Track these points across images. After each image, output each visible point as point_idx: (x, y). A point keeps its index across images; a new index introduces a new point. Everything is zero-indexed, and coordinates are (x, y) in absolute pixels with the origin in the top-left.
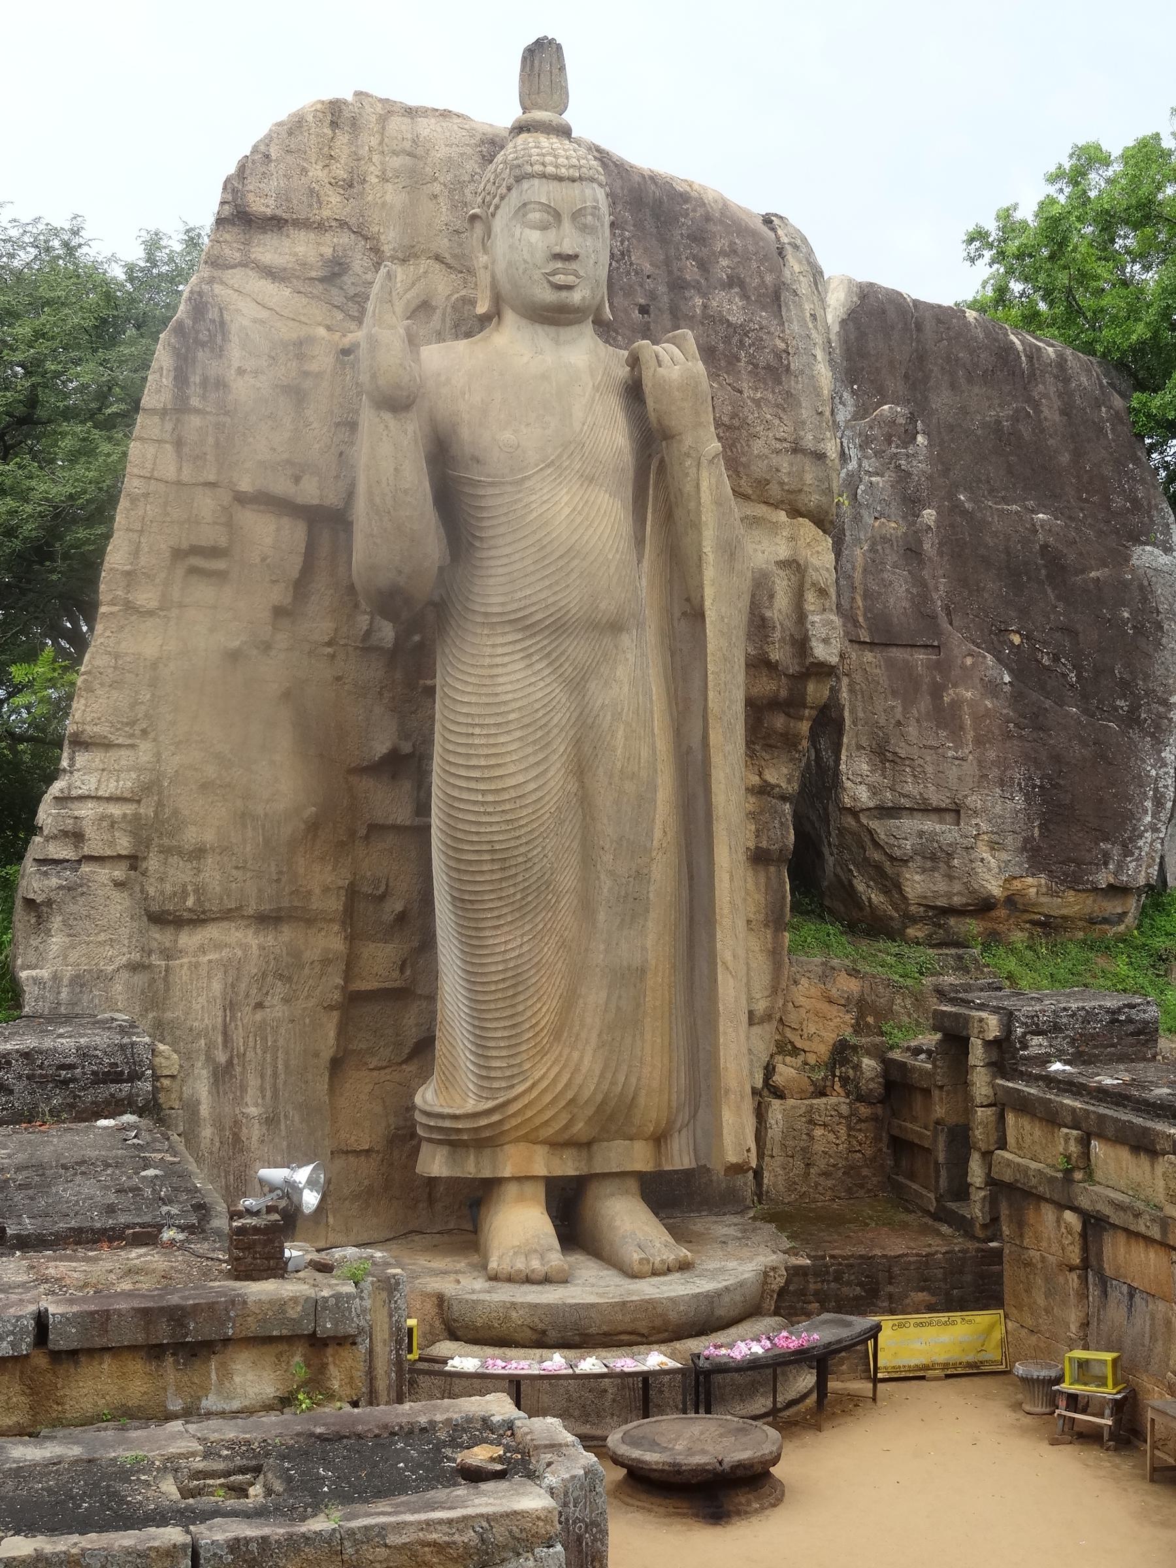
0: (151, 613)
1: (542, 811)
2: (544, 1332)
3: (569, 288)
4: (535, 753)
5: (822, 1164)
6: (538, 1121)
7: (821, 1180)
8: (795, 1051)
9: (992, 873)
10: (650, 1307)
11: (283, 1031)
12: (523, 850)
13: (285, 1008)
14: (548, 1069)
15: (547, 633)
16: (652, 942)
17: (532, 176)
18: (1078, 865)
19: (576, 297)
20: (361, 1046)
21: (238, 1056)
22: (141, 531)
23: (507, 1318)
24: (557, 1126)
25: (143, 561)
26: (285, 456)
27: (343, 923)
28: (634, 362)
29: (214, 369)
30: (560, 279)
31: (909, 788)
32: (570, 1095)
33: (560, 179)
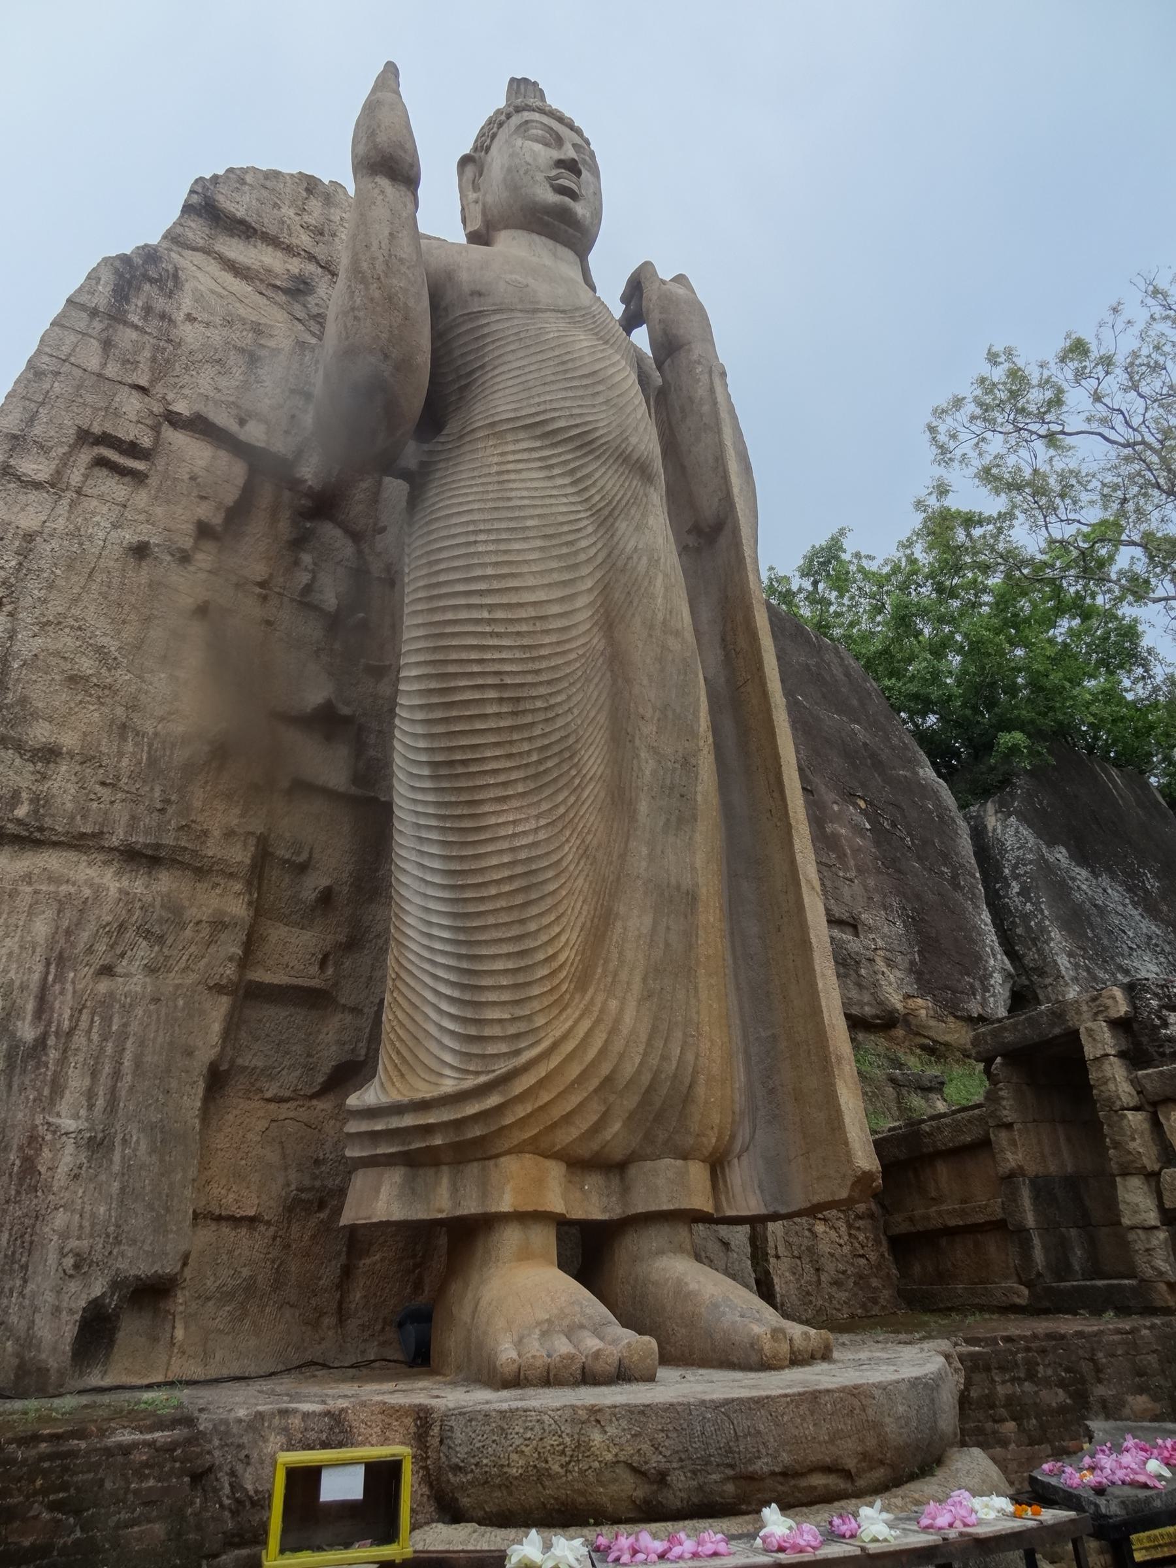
0: (37, 485)
1: (567, 647)
2: (661, 1479)
4: (560, 570)
5: (830, 1267)
6: (557, 1113)
7: (834, 1290)
10: (856, 1403)
11: (139, 1012)
12: (542, 691)
13: (148, 980)
14: (576, 1023)
15: (570, 446)
18: (954, 992)
20: (254, 1062)
21: (57, 1034)
22: (42, 404)
23: (582, 1446)
24: (583, 1124)
25: (38, 430)
26: (232, 399)
27: (249, 883)
29: (160, 303)
32: (605, 1069)
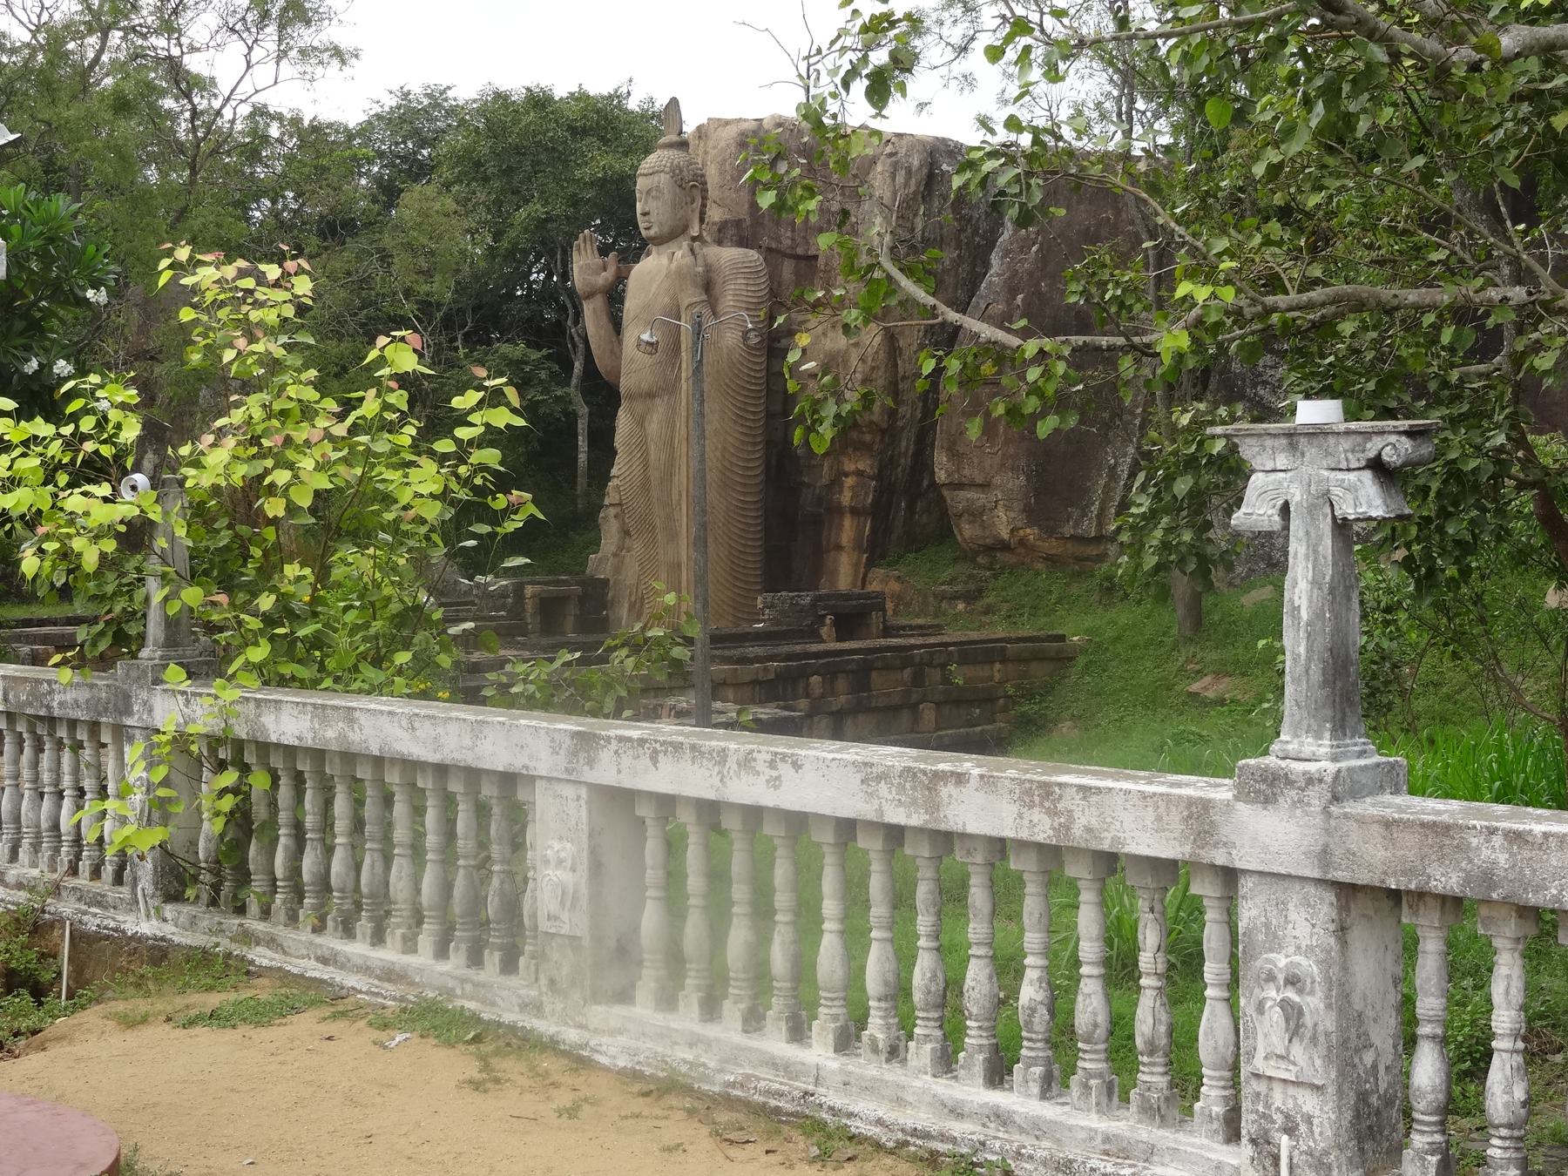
9: (1003, 523)
31: (966, 472)
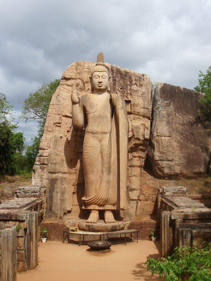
0: (50, 132)
3: (101, 86)
8: (143, 194)
16: (113, 178)
17: (95, 71)
19: (102, 88)
28: (111, 96)
30: (99, 85)
33: (100, 72)
